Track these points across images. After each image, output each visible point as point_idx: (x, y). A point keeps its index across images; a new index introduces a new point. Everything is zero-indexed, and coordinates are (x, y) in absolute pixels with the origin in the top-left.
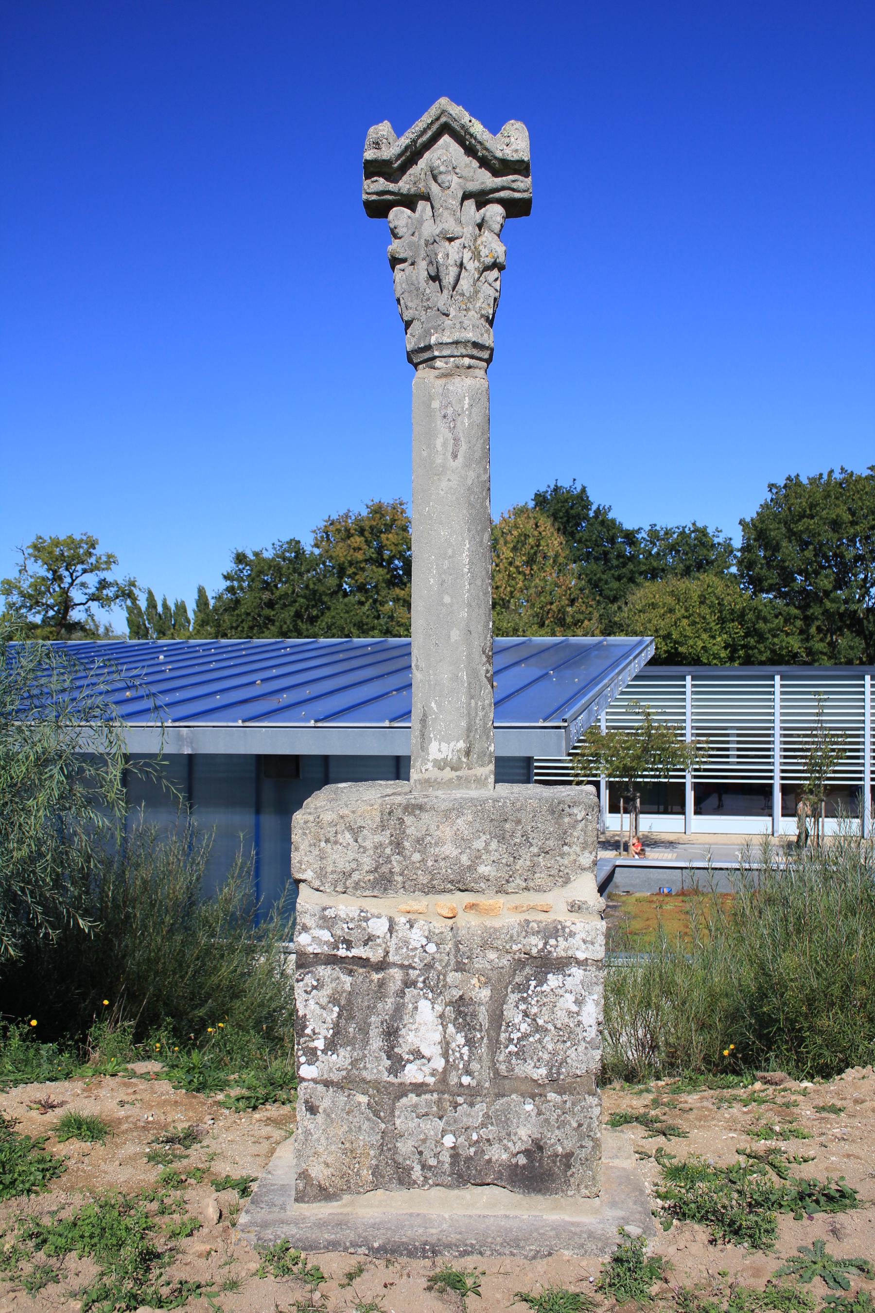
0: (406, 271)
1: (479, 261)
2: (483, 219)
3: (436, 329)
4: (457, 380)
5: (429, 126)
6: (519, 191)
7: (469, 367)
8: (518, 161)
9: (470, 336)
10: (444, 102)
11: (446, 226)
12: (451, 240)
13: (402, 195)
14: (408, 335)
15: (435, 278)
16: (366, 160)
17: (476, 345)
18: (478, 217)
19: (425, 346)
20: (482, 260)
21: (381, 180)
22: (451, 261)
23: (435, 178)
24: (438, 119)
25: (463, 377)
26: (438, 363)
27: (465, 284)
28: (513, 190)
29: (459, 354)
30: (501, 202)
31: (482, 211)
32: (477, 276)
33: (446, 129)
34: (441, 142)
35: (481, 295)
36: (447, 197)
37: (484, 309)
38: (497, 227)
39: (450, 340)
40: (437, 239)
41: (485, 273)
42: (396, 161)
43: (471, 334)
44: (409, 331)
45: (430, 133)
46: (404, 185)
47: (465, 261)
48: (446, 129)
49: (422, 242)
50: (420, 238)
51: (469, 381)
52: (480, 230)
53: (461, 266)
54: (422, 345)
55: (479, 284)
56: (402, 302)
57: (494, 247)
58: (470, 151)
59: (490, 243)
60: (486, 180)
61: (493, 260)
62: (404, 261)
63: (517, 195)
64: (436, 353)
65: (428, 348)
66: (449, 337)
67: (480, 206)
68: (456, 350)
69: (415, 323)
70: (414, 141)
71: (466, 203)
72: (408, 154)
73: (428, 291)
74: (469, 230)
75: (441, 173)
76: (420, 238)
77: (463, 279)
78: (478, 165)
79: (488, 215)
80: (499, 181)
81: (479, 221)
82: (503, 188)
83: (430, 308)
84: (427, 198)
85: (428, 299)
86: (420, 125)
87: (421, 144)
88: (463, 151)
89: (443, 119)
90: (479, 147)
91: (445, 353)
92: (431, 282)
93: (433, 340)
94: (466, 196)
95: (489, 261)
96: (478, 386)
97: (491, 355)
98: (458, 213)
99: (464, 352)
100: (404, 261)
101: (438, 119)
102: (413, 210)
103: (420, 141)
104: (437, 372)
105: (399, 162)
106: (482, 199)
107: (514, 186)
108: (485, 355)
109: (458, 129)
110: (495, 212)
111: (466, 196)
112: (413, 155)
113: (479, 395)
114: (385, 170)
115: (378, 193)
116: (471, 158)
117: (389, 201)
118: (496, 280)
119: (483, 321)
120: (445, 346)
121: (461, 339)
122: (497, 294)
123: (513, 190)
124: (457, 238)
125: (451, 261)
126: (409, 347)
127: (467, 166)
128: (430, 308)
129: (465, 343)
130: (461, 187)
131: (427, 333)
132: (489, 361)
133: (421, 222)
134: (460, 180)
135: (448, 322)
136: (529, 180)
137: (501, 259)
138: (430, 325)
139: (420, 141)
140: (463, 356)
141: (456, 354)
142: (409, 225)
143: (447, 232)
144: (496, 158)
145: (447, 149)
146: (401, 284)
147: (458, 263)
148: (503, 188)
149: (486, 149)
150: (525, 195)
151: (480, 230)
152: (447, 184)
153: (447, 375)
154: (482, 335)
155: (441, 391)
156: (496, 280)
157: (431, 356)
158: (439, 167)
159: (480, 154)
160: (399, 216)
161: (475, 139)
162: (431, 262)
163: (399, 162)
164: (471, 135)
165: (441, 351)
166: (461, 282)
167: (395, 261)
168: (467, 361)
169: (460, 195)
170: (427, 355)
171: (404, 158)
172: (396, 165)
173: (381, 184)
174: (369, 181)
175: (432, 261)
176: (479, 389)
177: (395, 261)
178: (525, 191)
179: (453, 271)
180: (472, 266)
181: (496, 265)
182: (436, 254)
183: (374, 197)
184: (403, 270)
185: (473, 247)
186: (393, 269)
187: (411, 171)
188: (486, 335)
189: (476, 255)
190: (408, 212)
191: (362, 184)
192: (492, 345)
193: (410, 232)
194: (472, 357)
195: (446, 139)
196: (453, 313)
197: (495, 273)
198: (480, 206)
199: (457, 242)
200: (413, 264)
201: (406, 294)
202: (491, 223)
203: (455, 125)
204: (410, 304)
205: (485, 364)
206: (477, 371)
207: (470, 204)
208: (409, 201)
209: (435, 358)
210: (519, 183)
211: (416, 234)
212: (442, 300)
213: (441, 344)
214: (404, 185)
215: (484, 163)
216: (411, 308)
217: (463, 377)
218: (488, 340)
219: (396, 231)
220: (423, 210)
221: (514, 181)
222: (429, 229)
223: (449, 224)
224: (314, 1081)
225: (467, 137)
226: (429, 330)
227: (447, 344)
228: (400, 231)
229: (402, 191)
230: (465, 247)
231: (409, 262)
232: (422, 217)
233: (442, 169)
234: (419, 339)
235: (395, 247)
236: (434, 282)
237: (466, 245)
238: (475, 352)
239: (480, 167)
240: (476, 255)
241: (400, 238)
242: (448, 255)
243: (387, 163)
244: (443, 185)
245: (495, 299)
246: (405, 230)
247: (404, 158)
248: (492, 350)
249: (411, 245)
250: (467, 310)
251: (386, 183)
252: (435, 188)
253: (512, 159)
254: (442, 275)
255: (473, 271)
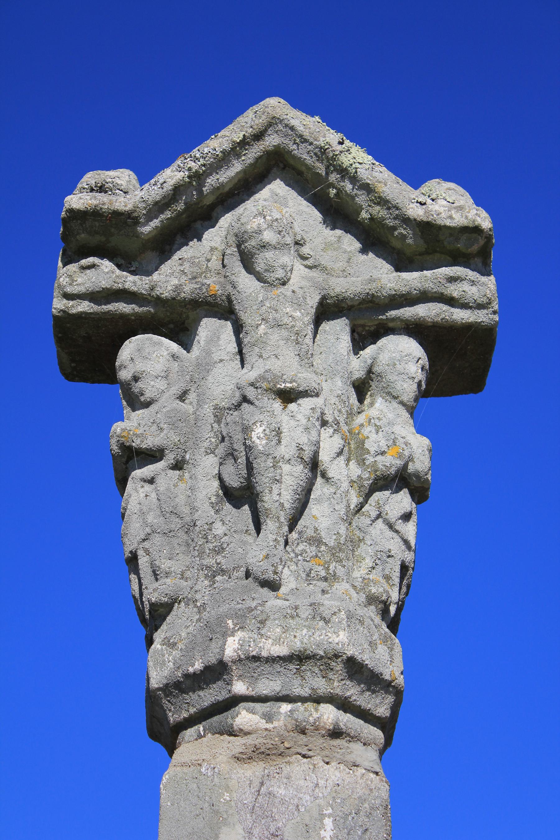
0: (159, 480)
1: (361, 462)
2: (370, 371)
3: (242, 619)
4: (297, 768)
5: (244, 143)
6: (465, 306)
7: (336, 733)
8: (465, 230)
9: (340, 639)
10: (275, 105)
11: (274, 365)
12: (288, 396)
13: (159, 301)
14: (157, 646)
15: (242, 495)
16: (71, 211)
17: (355, 669)
18: (357, 366)
19: (207, 669)
20: (370, 460)
21: (106, 265)
22: (286, 450)
23: (247, 261)
24: (259, 136)
25: (317, 760)
26: (244, 717)
27: (322, 515)
28: (451, 301)
29: (305, 692)
30: (416, 330)
31: (370, 350)
32: (355, 500)
33: (277, 165)
34: (265, 193)
35: (366, 551)
36: (279, 308)
37: (375, 583)
38: (408, 390)
39: (281, 650)
40: (251, 393)
41: (377, 496)
42: (150, 217)
43: (343, 637)
44: (159, 636)
45: (236, 167)
46: (170, 278)
47: (324, 457)
48: (277, 165)
49: (208, 410)
50: (200, 404)
51: (334, 774)
52: (361, 400)
53: (314, 465)
54: (198, 666)
55: (362, 521)
56: (143, 561)
57: (397, 435)
58: (337, 213)
59: (391, 424)
60: (377, 275)
61: (399, 463)
62: (152, 456)
63: (461, 316)
64: (240, 687)
65: (217, 671)
66: (278, 641)
67: (361, 339)
68: (297, 682)
69: (179, 610)
70: (198, 178)
71: (326, 326)
72: (180, 206)
73: (219, 529)
74: (334, 392)
75: (264, 246)
76: (200, 404)
77: (319, 501)
78: (358, 245)
79: (384, 359)
80: (413, 280)
81: (359, 374)
82: (424, 297)
83: (223, 572)
84: (225, 310)
85: (219, 550)
86: (217, 144)
87: (215, 190)
88: (317, 215)
89: (272, 141)
90: (362, 199)
91: (267, 686)
92: (228, 507)
93: (232, 647)
94: (327, 311)
95: (389, 463)
96: (360, 791)
97: (395, 709)
98: (308, 340)
99: (321, 686)
100: (152, 456)
101: (259, 136)
102: (187, 346)
103: (211, 181)
104: (237, 744)
105: (155, 223)
106: (368, 320)
107: (454, 290)
108: (381, 706)
109: (309, 160)
110: (403, 358)
111: (327, 311)
112: (192, 216)
113: (362, 819)
114: (117, 240)
115: (94, 296)
116: (338, 232)
117: (123, 316)
118: (406, 517)
119: (372, 613)
120: (267, 668)
121: (312, 649)
122: (409, 557)
123: (451, 301)
124: (305, 394)
125: (286, 450)
126: (157, 678)
127: (327, 246)
128: (223, 572)
129: (325, 660)
130: (316, 285)
131: (216, 631)
132: (387, 725)
133: (205, 367)
134: (314, 274)
135: (273, 602)
136: (490, 282)
137: (421, 463)
138: (224, 608)
139: (211, 181)
140: (317, 700)
141: (297, 691)
142: (173, 376)
143: (277, 378)
144: (406, 221)
145: (278, 206)
146: (142, 513)
147: (307, 455)
148: (424, 297)
149: (383, 202)
150: (482, 317)
151: (361, 400)
152: (280, 274)
153: (264, 753)
154: (372, 645)
155: (249, 799)
156: (406, 517)
157: (222, 696)
158: (259, 232)
159: (364, 215)
160: (145, 356)
161: (354, 179)
162: (231, 454)
163: (155, 223)
164: (343, 172)
165: (253, 681)
166: (313, 509)
167: (133, 457)
168: (329, 714)
169: (313, 301)
170: (208, 696)
171: (168, 214)
172: (147, 229)
173: (105, 273)
174: (73, 267)
175: (239, 452)
176: (362, 800)
177: (133, 457)
178: (480, 306)
179: (293, 475)
180: (341, 471)
181: (400, 480)
182: (246, 430)
183: (84, 307)
184: (151, 481)
185: (345, 428)
186: (122, 482)
187: (185, 252)
188: (382, 649)
189: (354, 448)
190: (174, 347)
191: (53, 276)
192: (400, 680)
193: (176, 390)
194: (344, 705)
195: (277, 187)
196: (289, 581)
197: (402, 501)
198: (361, 339)
199: (306, 403)
200: (178, 466)
201: (157, 539)
202: (392, 377)
203: (302, 153)
204: (165, 565)
205: (378, 734)
206: (357, 747)
207: (338, 331)
208: (176, 321)
209: (234, 702)
210: (465, 286)
211: (192, 397)
212: (258, 551)
213: (256, 658)
214: (170, 278)
215: (374, 239)
216: (167, 571)
217: (317, 760)
218: (388, 659)
219: (136, 388)
220: (214, 339)
221: (452, 280)
222: (225, 379)
223: (287, 367)
224: (314, 756)
225: (333, 177)
226: (221, 620)
227: (272, 660)
228: (149, 388)
229: (158, 291)
230: (324, 423)
231: (170, 458)
232: (208, 353)
233: (268, 236)
234: (189, 654)
235: (134, 426)
236: (237, 505)
237: (329, 418)
238: (353, 691)
239: (363, 251)
240: (354, 448)
241: (147, 405)
242: (278, 433)
243: (125, 220)
244: (271, 277)
245: (404, 568)
246: (161, 384)
247: (168, 214)
248: (398, 693)
249: (175, 421)
250: (330, 578)
251: (118, 272)
252: (246, 283)
253: (448, 223)
254: (262, 481)
255: (345, 485)
